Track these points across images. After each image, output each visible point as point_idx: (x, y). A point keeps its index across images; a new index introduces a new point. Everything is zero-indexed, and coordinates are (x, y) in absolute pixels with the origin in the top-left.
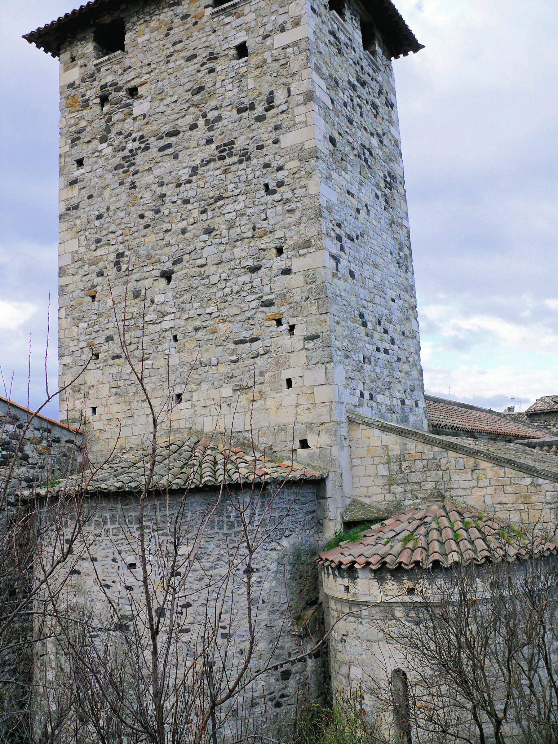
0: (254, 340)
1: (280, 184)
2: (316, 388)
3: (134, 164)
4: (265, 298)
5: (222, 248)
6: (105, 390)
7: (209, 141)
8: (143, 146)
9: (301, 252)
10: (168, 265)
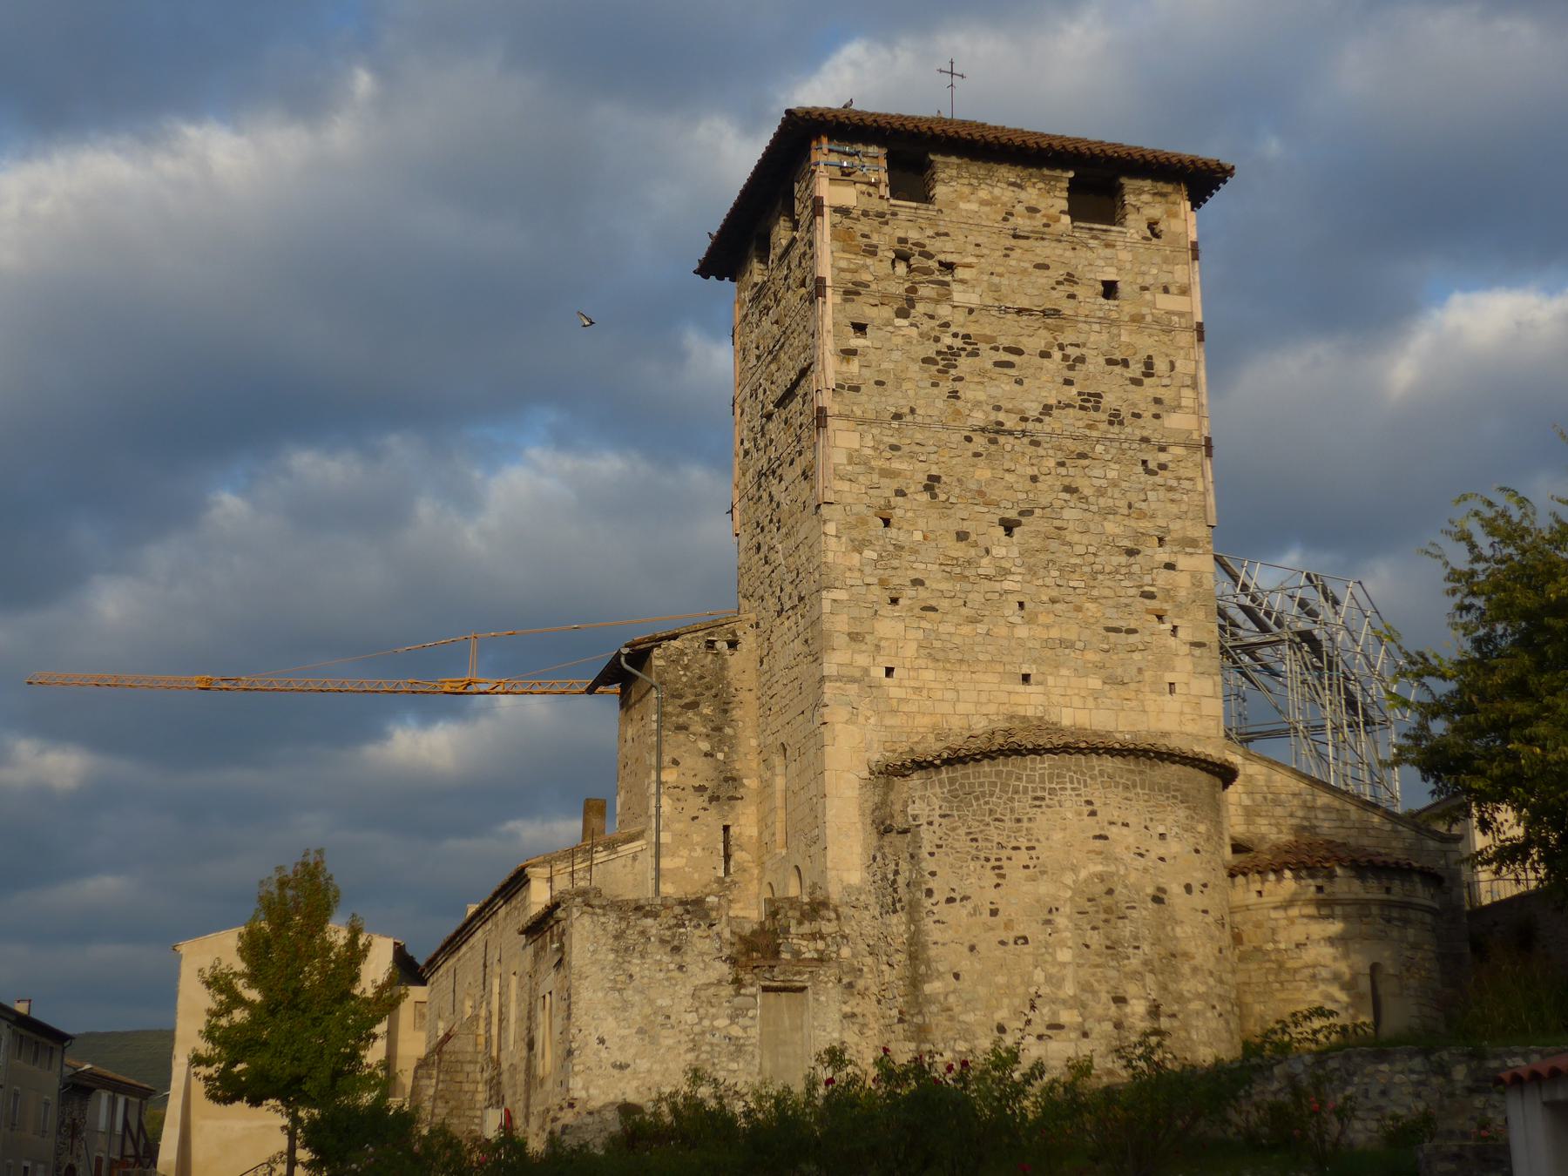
0: (1134, 631)
1: (1163, 467)
2: (1204, 700)
3: (955, 367)
4: (1146, 588)
5: (1089, 515)
6: (911, 650)
7: (1068, 382)
8: (969, 348)
9: (1188, 550)
10: (1012, 514)
